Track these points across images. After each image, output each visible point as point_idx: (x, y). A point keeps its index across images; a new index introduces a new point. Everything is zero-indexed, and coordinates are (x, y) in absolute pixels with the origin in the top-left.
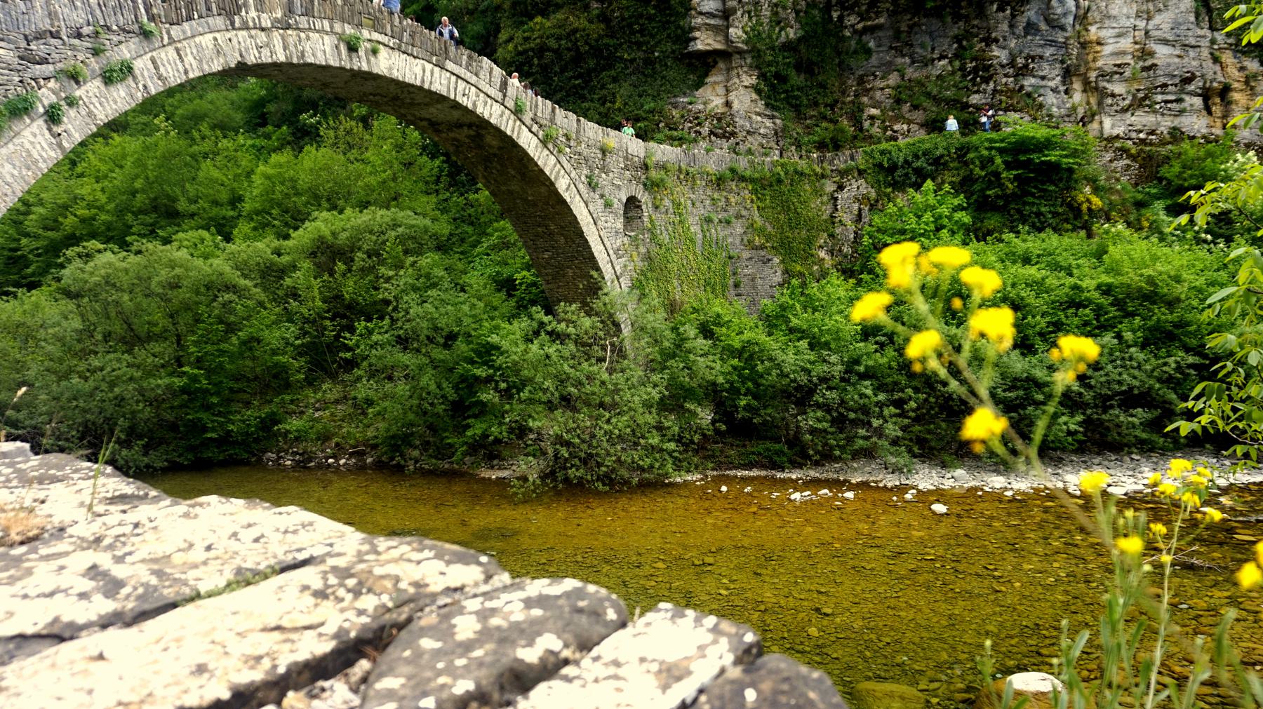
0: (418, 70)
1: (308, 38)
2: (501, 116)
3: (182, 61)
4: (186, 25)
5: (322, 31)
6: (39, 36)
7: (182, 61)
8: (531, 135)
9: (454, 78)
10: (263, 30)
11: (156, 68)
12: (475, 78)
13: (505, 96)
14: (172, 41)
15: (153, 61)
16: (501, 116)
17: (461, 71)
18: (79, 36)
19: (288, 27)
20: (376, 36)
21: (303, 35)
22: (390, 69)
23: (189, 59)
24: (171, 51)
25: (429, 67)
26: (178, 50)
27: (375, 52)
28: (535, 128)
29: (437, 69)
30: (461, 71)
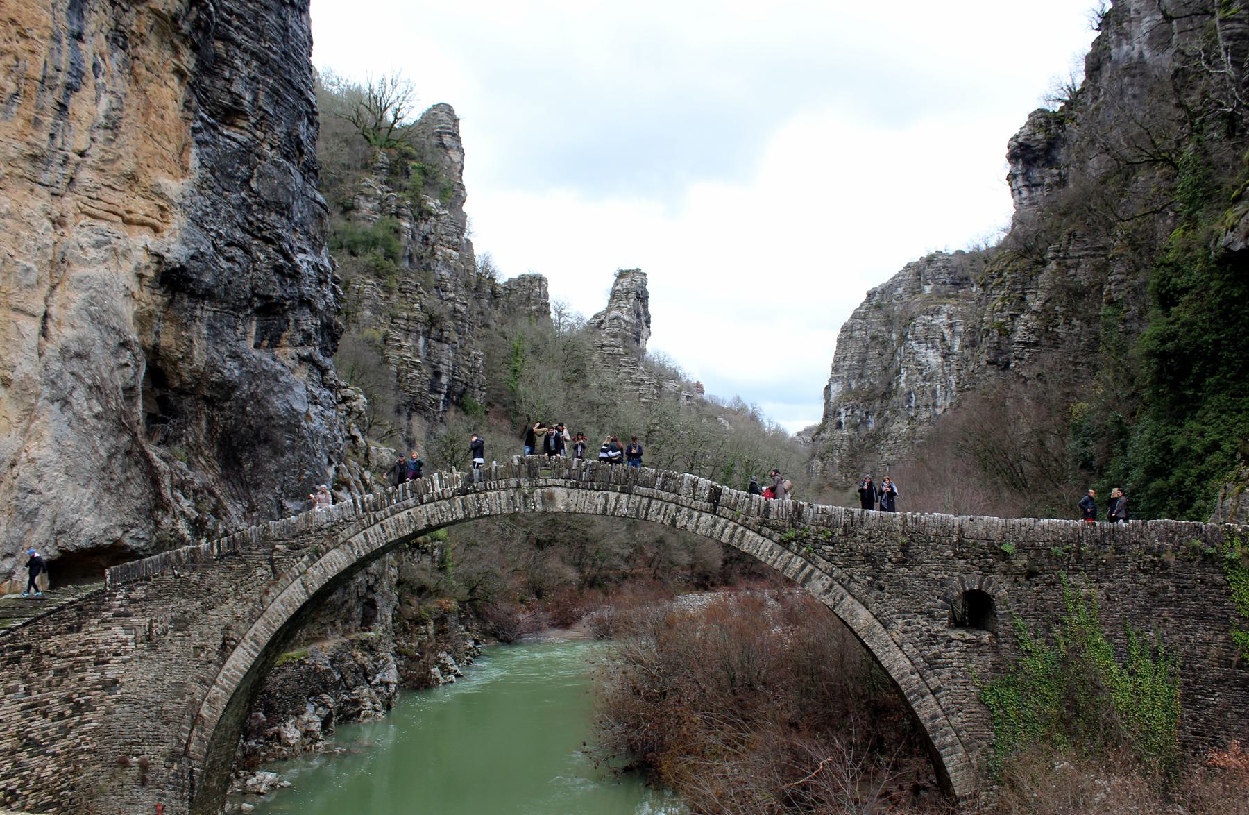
0: (601, 500)
1: (486, 497)
2: (714, 525)
3: (384, 531)
4: (387, 510)
5: (498, 489)
6: (302, 533)
7: (384, 531)
8: (761, 539)
9: (645, 501)
10: (448, 499)
11: (367, 539)
12: (672, 496)
13: (716, 505)
14: (376, 521)
15: (365, 535)
16: (714, 525)
17: (655, 492)
18: (320, 529)
19: (467, 493)
20: (551, 481)
21: (482, 495)
22: (567, 505)
23: (390, 530)
24: (377, 526)
25: (613, 496)
26: (382, 526)
27: (551, 497)
28: (766, 530)
29: (624, 497)
30: (655, 492)
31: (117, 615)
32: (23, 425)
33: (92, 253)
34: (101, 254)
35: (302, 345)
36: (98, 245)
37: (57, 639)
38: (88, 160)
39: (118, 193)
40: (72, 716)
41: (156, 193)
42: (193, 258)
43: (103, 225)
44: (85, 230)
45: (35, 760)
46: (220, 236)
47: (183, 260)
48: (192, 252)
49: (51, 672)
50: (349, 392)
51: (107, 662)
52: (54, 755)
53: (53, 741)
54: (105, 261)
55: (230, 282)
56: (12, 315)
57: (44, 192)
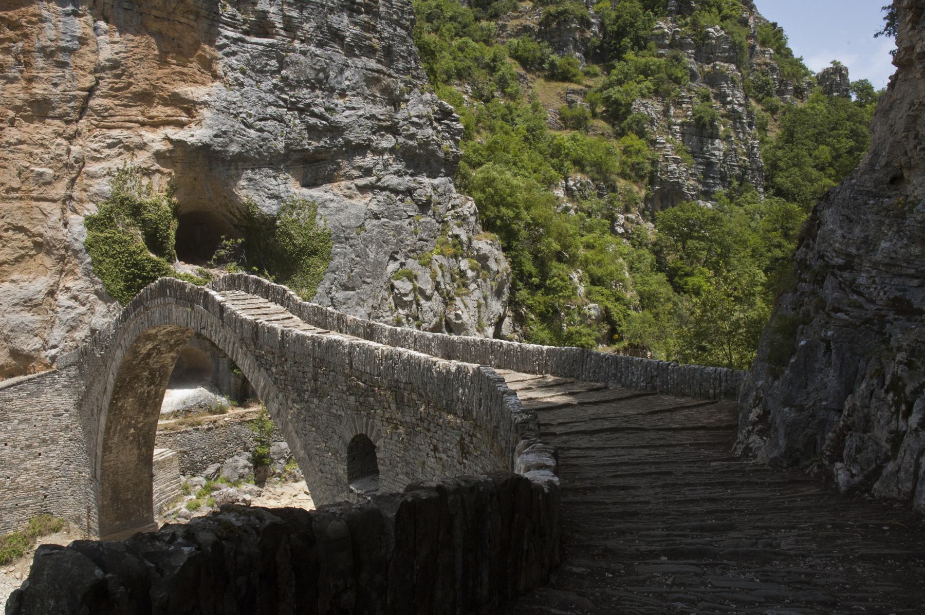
31: (64, 386)
32: (58, 267)
33: (107, 151)
34: (116, 150)
35: (360, 177)
36: (110, 146)
37: (18, 402)
38: (98, 92)
39: (134, 109)
40: (39, 446)
41: (176, 100)
42: (216, 136)
43: (115, 133)
44: (97, 139)
45: (9, 472)
46: (250, 115)
47: (206, 140)
48: (215, 132)
49: (16, 421)
50: (457, 202)
51: (62, 415)
52: (26, 470)
53: (23, 461)
54: (120, 154)
55: (261, 147)
56: (34, 203)
57: (57, 122)
